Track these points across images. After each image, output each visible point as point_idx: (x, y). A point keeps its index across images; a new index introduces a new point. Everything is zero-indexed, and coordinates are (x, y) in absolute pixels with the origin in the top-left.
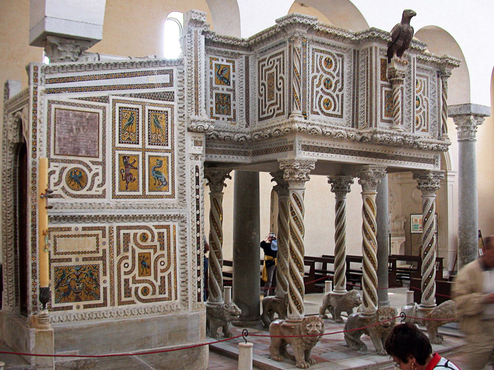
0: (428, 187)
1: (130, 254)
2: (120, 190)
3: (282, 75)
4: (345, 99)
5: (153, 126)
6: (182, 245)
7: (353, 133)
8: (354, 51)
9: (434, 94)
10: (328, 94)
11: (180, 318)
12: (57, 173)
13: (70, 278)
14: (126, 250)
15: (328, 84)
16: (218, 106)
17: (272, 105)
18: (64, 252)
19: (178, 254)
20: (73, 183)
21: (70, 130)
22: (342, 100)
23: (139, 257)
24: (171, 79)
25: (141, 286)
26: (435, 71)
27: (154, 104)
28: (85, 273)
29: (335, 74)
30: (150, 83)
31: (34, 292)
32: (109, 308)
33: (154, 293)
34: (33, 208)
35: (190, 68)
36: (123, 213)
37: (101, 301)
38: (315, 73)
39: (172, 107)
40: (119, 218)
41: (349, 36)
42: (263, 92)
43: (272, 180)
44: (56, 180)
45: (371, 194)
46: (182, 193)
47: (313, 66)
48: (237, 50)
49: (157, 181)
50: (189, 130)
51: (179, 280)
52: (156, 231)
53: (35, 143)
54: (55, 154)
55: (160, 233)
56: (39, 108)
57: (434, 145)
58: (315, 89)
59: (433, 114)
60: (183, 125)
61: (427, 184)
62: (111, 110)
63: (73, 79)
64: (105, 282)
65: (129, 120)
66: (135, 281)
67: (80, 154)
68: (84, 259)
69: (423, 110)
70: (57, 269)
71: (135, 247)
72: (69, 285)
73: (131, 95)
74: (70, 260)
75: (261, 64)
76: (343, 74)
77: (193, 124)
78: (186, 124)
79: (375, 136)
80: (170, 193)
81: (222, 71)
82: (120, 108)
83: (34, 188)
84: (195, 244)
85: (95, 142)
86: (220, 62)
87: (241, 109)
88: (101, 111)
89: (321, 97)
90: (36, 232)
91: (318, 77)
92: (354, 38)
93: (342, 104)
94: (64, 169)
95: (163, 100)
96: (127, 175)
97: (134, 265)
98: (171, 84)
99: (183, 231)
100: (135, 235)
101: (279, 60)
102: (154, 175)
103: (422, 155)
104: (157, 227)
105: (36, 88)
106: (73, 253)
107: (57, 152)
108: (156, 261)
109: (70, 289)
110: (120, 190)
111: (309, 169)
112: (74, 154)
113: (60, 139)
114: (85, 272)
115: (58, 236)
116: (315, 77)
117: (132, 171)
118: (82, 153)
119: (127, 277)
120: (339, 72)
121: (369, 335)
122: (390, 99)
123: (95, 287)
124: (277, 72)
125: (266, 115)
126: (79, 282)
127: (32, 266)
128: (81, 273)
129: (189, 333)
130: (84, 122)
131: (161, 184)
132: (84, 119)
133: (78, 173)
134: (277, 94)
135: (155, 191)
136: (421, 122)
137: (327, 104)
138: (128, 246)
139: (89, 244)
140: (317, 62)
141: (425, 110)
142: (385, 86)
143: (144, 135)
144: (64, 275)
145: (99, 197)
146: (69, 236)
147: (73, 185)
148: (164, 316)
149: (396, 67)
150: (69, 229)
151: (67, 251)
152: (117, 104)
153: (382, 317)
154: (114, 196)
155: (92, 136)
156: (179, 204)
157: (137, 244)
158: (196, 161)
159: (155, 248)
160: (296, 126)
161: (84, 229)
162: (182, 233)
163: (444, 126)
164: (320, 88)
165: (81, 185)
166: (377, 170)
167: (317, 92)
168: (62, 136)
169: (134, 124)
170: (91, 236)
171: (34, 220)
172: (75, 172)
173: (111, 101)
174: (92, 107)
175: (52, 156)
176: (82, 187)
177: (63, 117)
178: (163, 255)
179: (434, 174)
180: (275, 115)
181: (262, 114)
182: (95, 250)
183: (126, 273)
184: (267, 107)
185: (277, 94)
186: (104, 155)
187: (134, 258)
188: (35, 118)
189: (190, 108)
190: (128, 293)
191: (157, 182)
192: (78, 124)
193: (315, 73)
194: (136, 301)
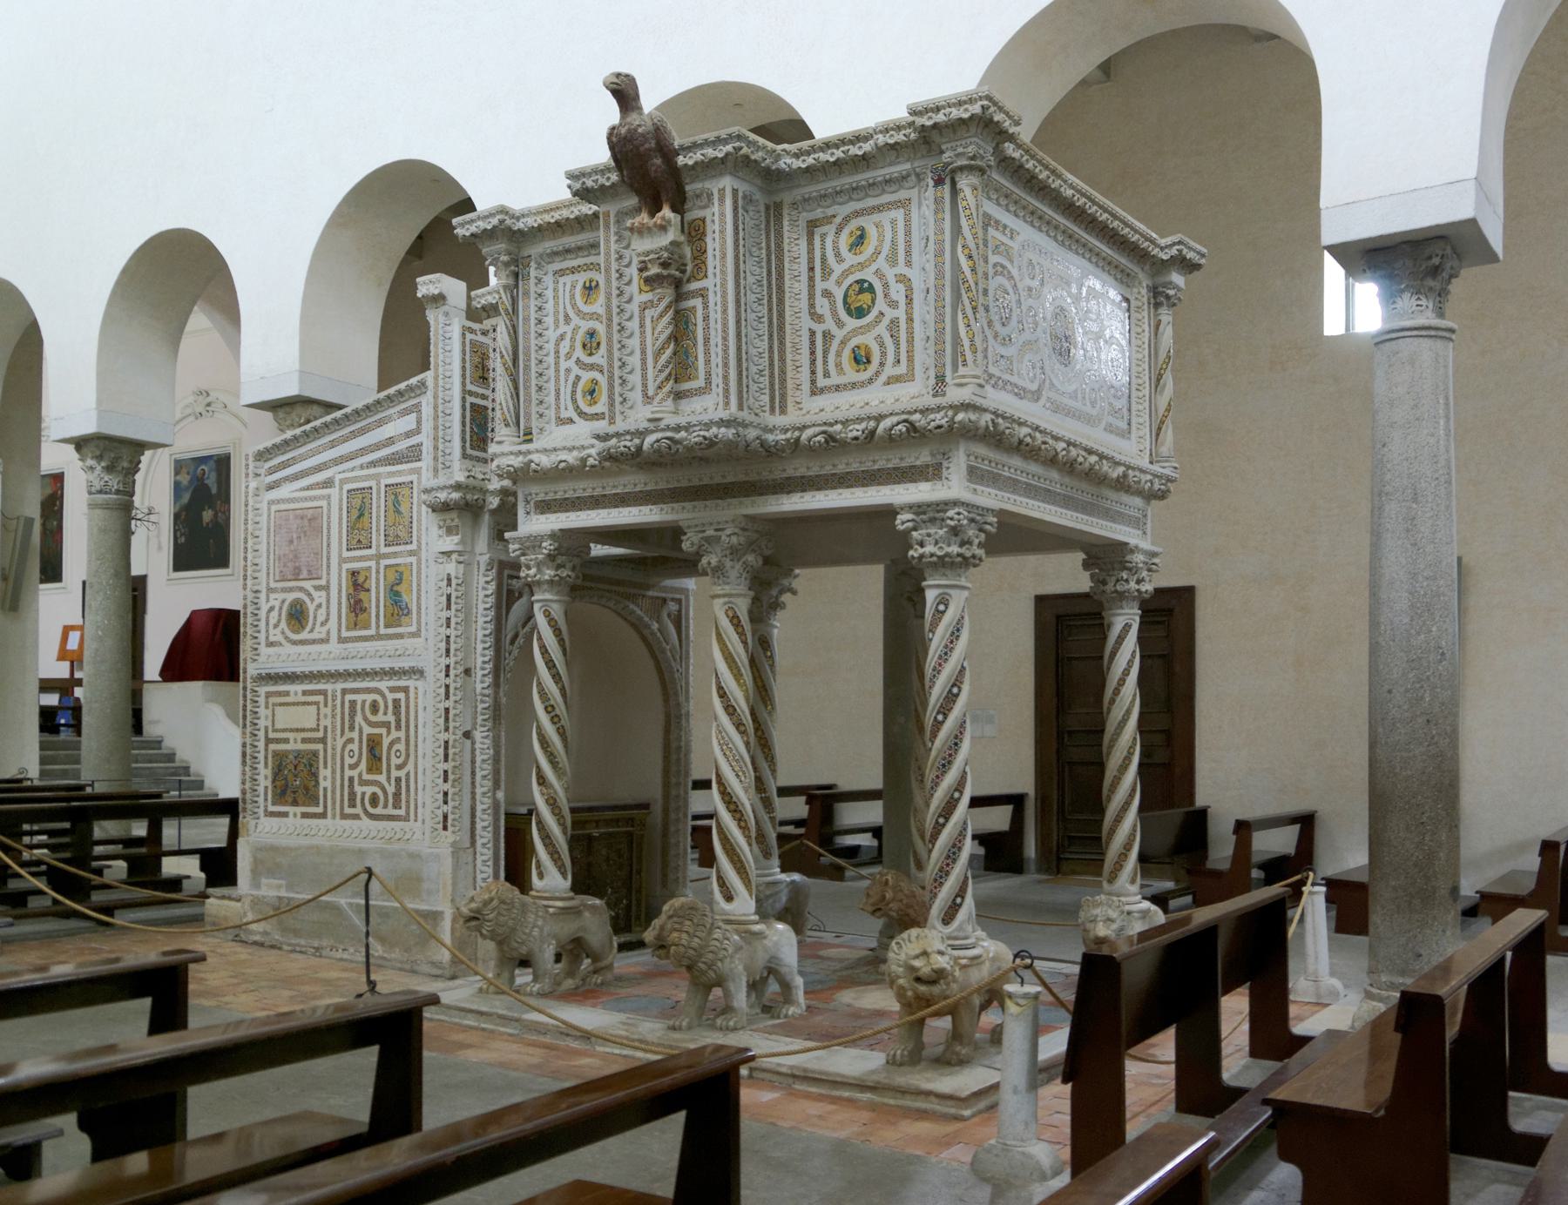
2: (348, 629)
11: (414, 856)
12: (277, 609)
14: (352, 728)
32: (328, 821)
33: (385, 806)
58: (563, 365)
62: (337, 496)
64: (325, 778)
68: (304, 741)
70: (276, 754)
73: (362, 467)
74: (286, 741)
89: (578, 378)
98: (417, 431)
103: (853, 463)
104: (393, 690)
106: (292, 730)
108: (390, 748)
110: (348, 629)
116: (562, 337)
129: (425, 886)
132: (306, 521)
136: (883, 354)
141: (901, 313)
157: (365, 719)
161: (305, 693)
164: (574, 359)
166: (710, 532)
167: (568, 371)
173: (337, 483)
179: (917, 514)
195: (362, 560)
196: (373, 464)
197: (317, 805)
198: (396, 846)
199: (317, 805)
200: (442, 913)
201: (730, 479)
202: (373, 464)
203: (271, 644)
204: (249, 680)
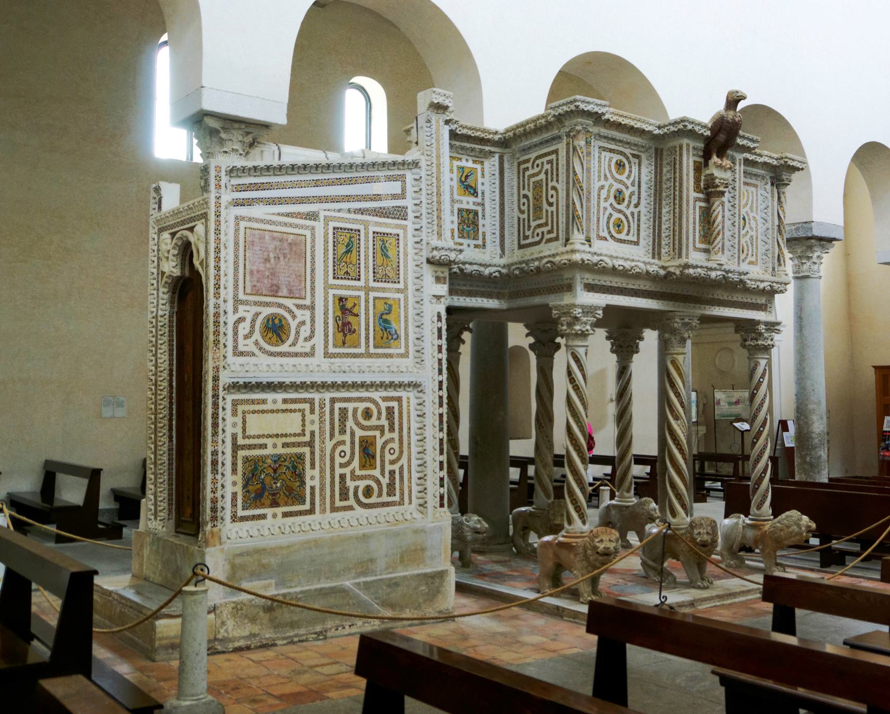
0: (758, 345)
1: (347, 437)
2: (335, 346)
3: (554, 183)
4: (643, 218)
5: (379, 255)
6: (419, 425)
7: (654, 266)
8: (656, 150)
9: (766, 211)
10: (620, 211)
11: (416, 532)
12: (248, 320)
13: (264, 472)
14: (343, 431)
15: (619, 197)
16: (461, 227)
17: (539, 226)
18: (256, 434)
19: (414, 438)
20: (270, 335)
21: (266, 260)
22: (639, 220)
23: (360, 442)
24: (404, 189)
25: (362, 484)
26: (768, 177)
27: (381, 223)
28: (285, 466)
29: (629, 183)
30: (375, 193)
31: (214, 493)
32: (317, 516)
34: (215, 370)
35: (429, 173)
36: (339, 379)
37: (307, 506)
38: (602, 182)
39: (404, 228)
40: (334, 386)
41: (650, 128)
42: (525, 208)
43: (527, 335)
44: (247, 331)
45: (677, 354)
46: (418, 351)
47: (599, 172)
48: (487, 146)
49: (385, 333)
50: (429, 261)
51: (415, 476)
52: (384, 405)
53: (217, 278)
54: (245, 294)
55: (389, 407)
56: (223, 227)
57: (766, 284)
58: (603, 204)
59: (765, 239)
60: (421, 254)
61: (757, 340)
62: (323, 231)
63: (269, 186)
64: (312, 478)
65: (347, 246)
66: (354, 477)
67: (280, 294)
68: (285, 445)
69: (751, 233)
70: (246, 460)
71: (355, 428)
72: (263, 483)
73: (349, 211)
75: (523, 167)
76: (639, 182)
77: (435, 253)
78: (425, 254)
79: (686, 271)
80: (402, 351)
81: (467, 177)
82: (334, 228)
83: (216, 342)
84: (437, 423)
85: (301, 278)
86: (463, 163)
87: (493, 231)
88: (308, 233)
89: (611, 215)
90: (218, 405)
91: (606, 188)
92: (657, 132)
93: (639, 226)
94: (257, 314)
95: (392, 218)
96: (344, 324)
97: (353, 453)
98: (403, 196)
99: (420, 404)
100: (355, 410)
101: (550, 162)
102: (380, 324)
103: (749, 299)
104: (385, 399)
105: (218, 198)
107: (248, 290)
108: (383, 448)
109: (263, 488)
110: (335, 346)
111: (595, 317)
112: (271, 294)
113: (252, 272)
114: (286, 463)
115: (249, 412)
116: (602, 187)
117: (350, 319)
118: (282, 292)
119: (343, 471)
120: (634, 180)
121: (678, 560)
122: (707, 218)
123: (299, 486)
124: (547, 179)
125: (530, 240)
126: (276, 479)
127: (212, 455)
128: (280, 465)
129: (428, 554)
130: (285, 249)
131: (390, 337)
132: (286, 244)
133: (277, 321)
134: (547, 211)
135: (382, 347)
136: (748, 250)
137: (619, 225)
138: (345, 426)
139: (291, 424)
140: (605, 165)
141: (754, 233)
142: (699, 200)
143: (366, 267)
144: (256, 468)
145: (306, 355)
146: (263, 412)
147: (270, 338)
148: (393, 528)
149: (717, 173)
150: (264, 402)
151: (261, 433)
152: (330, 223)
153: (698, 531)
154: (327, 355)
155: (297, 269)
156: (415, 366)
157: (358, 424)
158: (437, 305)
159: (381, 429)
160: (577, 257)
161: (285, 401)
162: (419, 407)
163: (781, 255)
165: (281, 339)
166: (687, 320)
167: (605, 209)
168: (255, 268)
169: (354, 252)
170: (295, 411)
171: (216, 388)
172: (273, 320)
173: (322, 218)
174: (297, 226)
175: (242, 296)
176: (282, 341)
177: (256, 240)
178: (392, 440)
180: (544, 240)
181: (524, 239)
182: (301, 432)
183: (342, 466)
184: (532, 228)
185: (547, 211)
186: (313, 295)
187: (353, 443)
188: (217, 241)
189: (430, 230)
190: (344, 496)
191: (385, 335)
192: (277, 251)
193: (602, 182)
194: (355, 506)
195: (348, 289)
196: (361, 211)
197: (304, 502)
198: (401, 526)
199: (304, 502)
200: (447, 570)
201: (690, 293)
202: (361, 211)
203: (238, 353)
204: (221, 389)
